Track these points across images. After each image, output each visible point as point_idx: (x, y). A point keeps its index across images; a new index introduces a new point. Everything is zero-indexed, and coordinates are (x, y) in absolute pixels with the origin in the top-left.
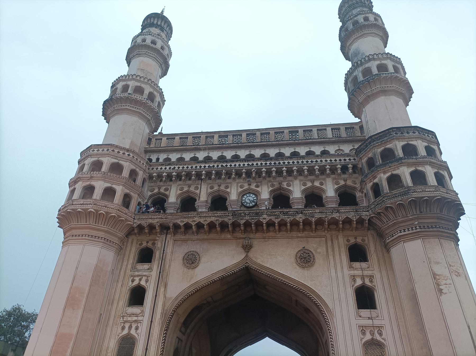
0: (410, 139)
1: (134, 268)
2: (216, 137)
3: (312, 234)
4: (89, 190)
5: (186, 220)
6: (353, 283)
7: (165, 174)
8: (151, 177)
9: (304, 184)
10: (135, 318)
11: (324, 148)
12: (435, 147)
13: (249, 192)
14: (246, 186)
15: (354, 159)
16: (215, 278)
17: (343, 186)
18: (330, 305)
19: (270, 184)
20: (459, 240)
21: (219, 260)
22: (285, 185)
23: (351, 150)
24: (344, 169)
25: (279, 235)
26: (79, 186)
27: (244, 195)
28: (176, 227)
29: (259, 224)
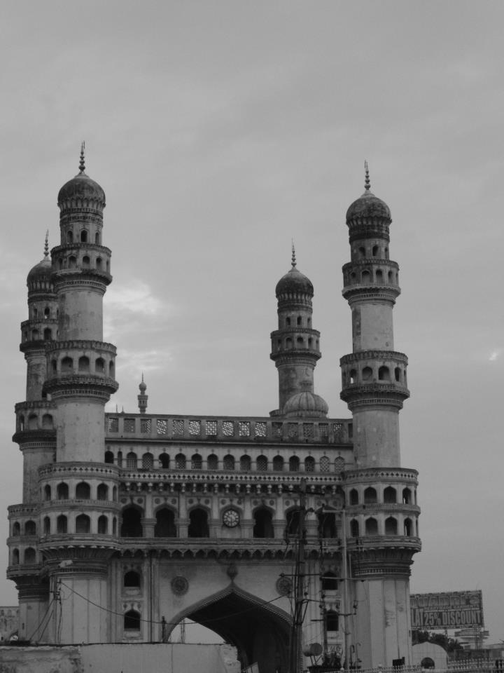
1: (123, 593)
2: (186, 421)
4: (83, 521)
5: (175, 547)
7: (139, 484)
8: (123, 485)
9: (287, 503)
11: (310, 453)
12: (412, 488)
13: (231, 508)
14: (228, 503)
15: (339, 479)
16: (205, 604)
19: (252, 500)
20: (410, 575)
22: (268, 502)
23: (337, 459)
24: (329, 488)
27: (225, 512)
28: (165, 553)
29: (247, 552)
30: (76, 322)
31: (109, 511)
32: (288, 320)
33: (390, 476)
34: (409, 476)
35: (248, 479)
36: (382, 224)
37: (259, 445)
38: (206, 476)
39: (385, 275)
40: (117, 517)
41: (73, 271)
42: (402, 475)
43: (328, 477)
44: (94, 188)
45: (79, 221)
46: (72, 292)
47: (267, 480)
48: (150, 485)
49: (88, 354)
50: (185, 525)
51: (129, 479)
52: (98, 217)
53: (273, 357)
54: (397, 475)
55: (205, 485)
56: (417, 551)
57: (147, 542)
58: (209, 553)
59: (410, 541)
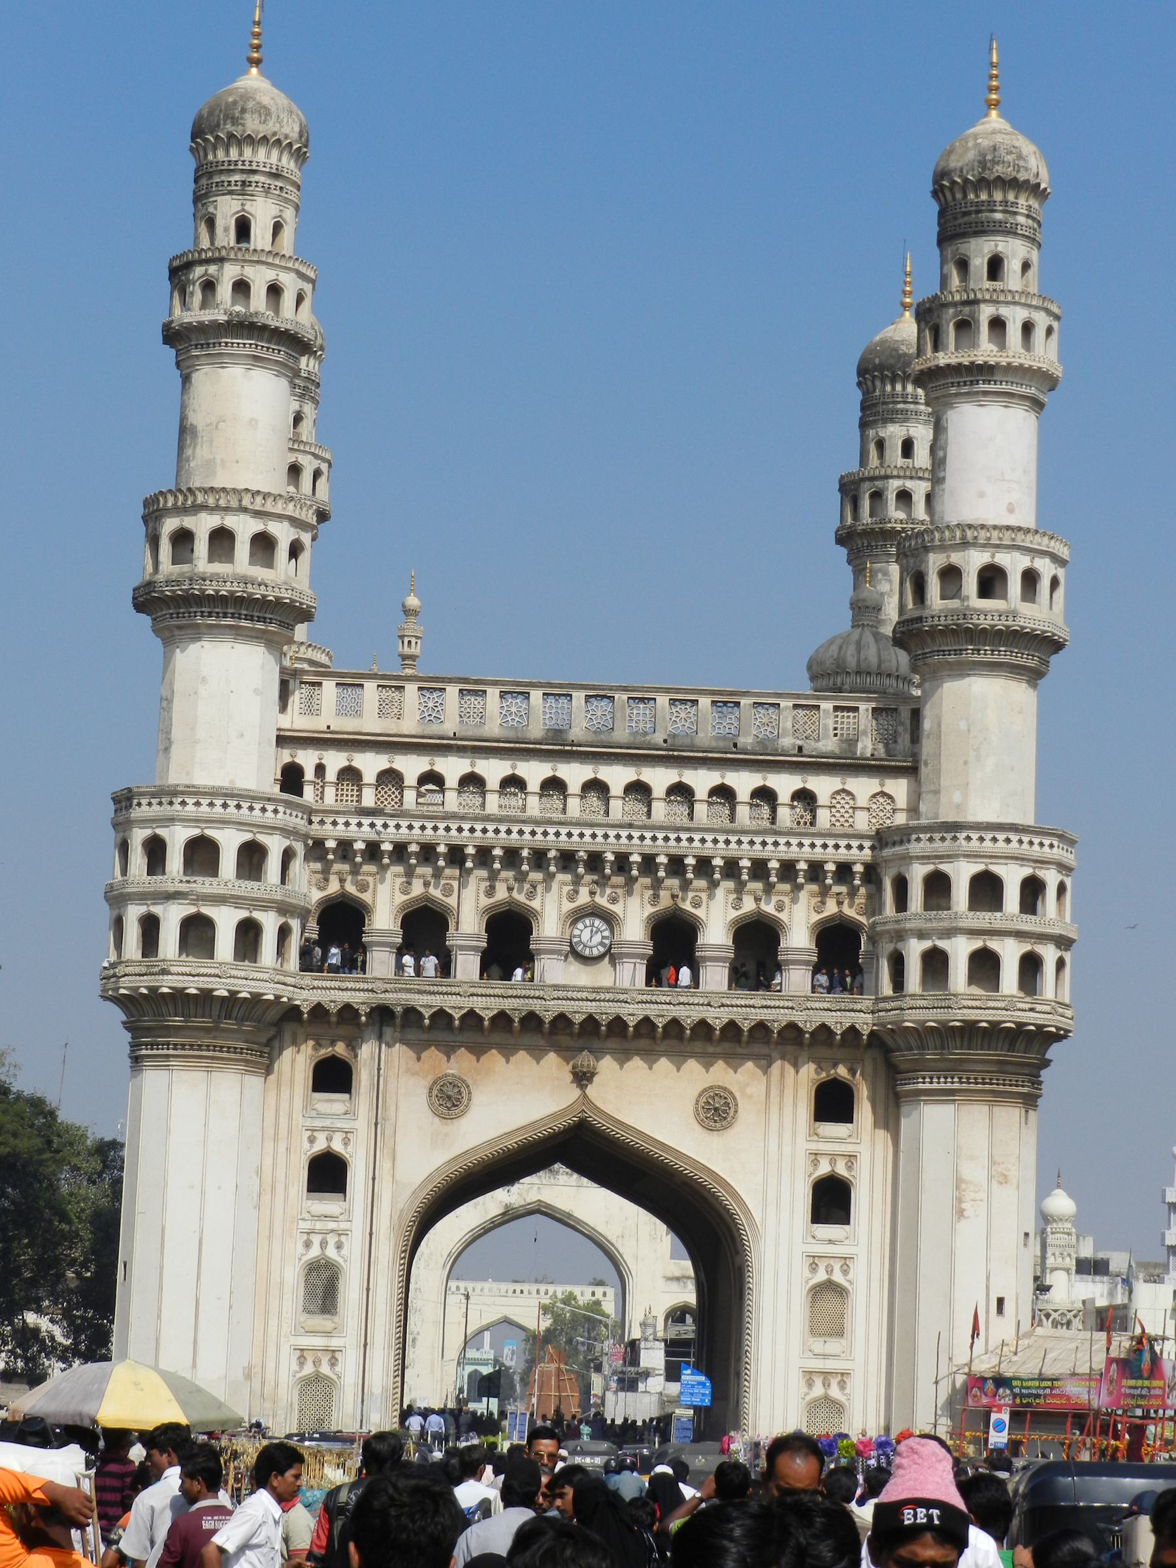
0: (993, 861)
3: (739, 1050)
5: (437, 1001)
6: (811, 1169)
10: (332, 1225)
14: (584, 898)
15: (872, 848)
16: (511, 1143)
17: (831, 918)
18: (757, 1215)
21: (518, 1098)
23: (874, 796)
24: (844, 871)
25: (662, 1047)
26: (172, 917)
28: (411, 1013)
29: (618, 1023)
30: (211, 442)
31: (265, 908)
32: (880, 444)
33: (988, 843)
34: (1041, 844)
35: (636, 841)
36: (1016, 198)
37: (673, 757)
38: (527, 829)
39: (1014, 333)
40: (295, 924)
41: (207, 316)
42: (1021, 842)
43: (843, 843)
44: (273, 109)
45: (231, 193)
46: (206, 369)
47: (684, 843)
48: (387, 847)
49: (231, 521)
50: (474, 949)
51: (331, 834)
52: (280, 184)
53: (841, 540)
54: (1008, 841)
55: (525, 853)
56: (1059, 1036)
57: (366, 986)
58: (523, 1020)
59: (1031, 1010)
